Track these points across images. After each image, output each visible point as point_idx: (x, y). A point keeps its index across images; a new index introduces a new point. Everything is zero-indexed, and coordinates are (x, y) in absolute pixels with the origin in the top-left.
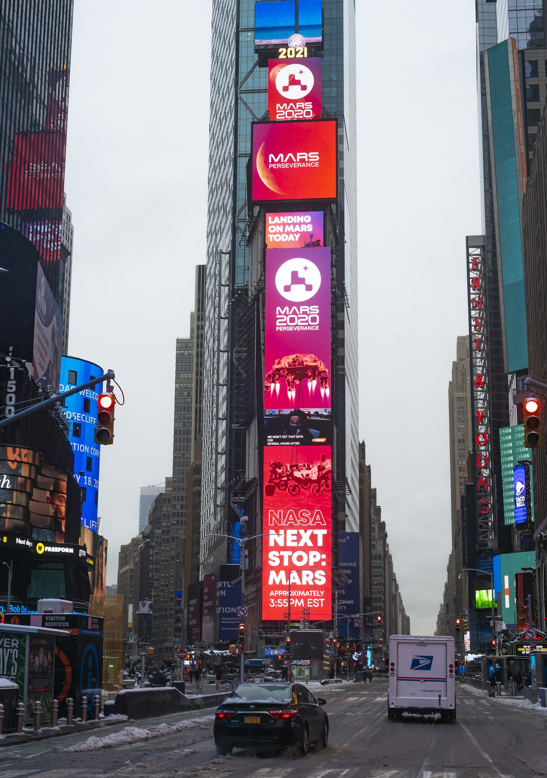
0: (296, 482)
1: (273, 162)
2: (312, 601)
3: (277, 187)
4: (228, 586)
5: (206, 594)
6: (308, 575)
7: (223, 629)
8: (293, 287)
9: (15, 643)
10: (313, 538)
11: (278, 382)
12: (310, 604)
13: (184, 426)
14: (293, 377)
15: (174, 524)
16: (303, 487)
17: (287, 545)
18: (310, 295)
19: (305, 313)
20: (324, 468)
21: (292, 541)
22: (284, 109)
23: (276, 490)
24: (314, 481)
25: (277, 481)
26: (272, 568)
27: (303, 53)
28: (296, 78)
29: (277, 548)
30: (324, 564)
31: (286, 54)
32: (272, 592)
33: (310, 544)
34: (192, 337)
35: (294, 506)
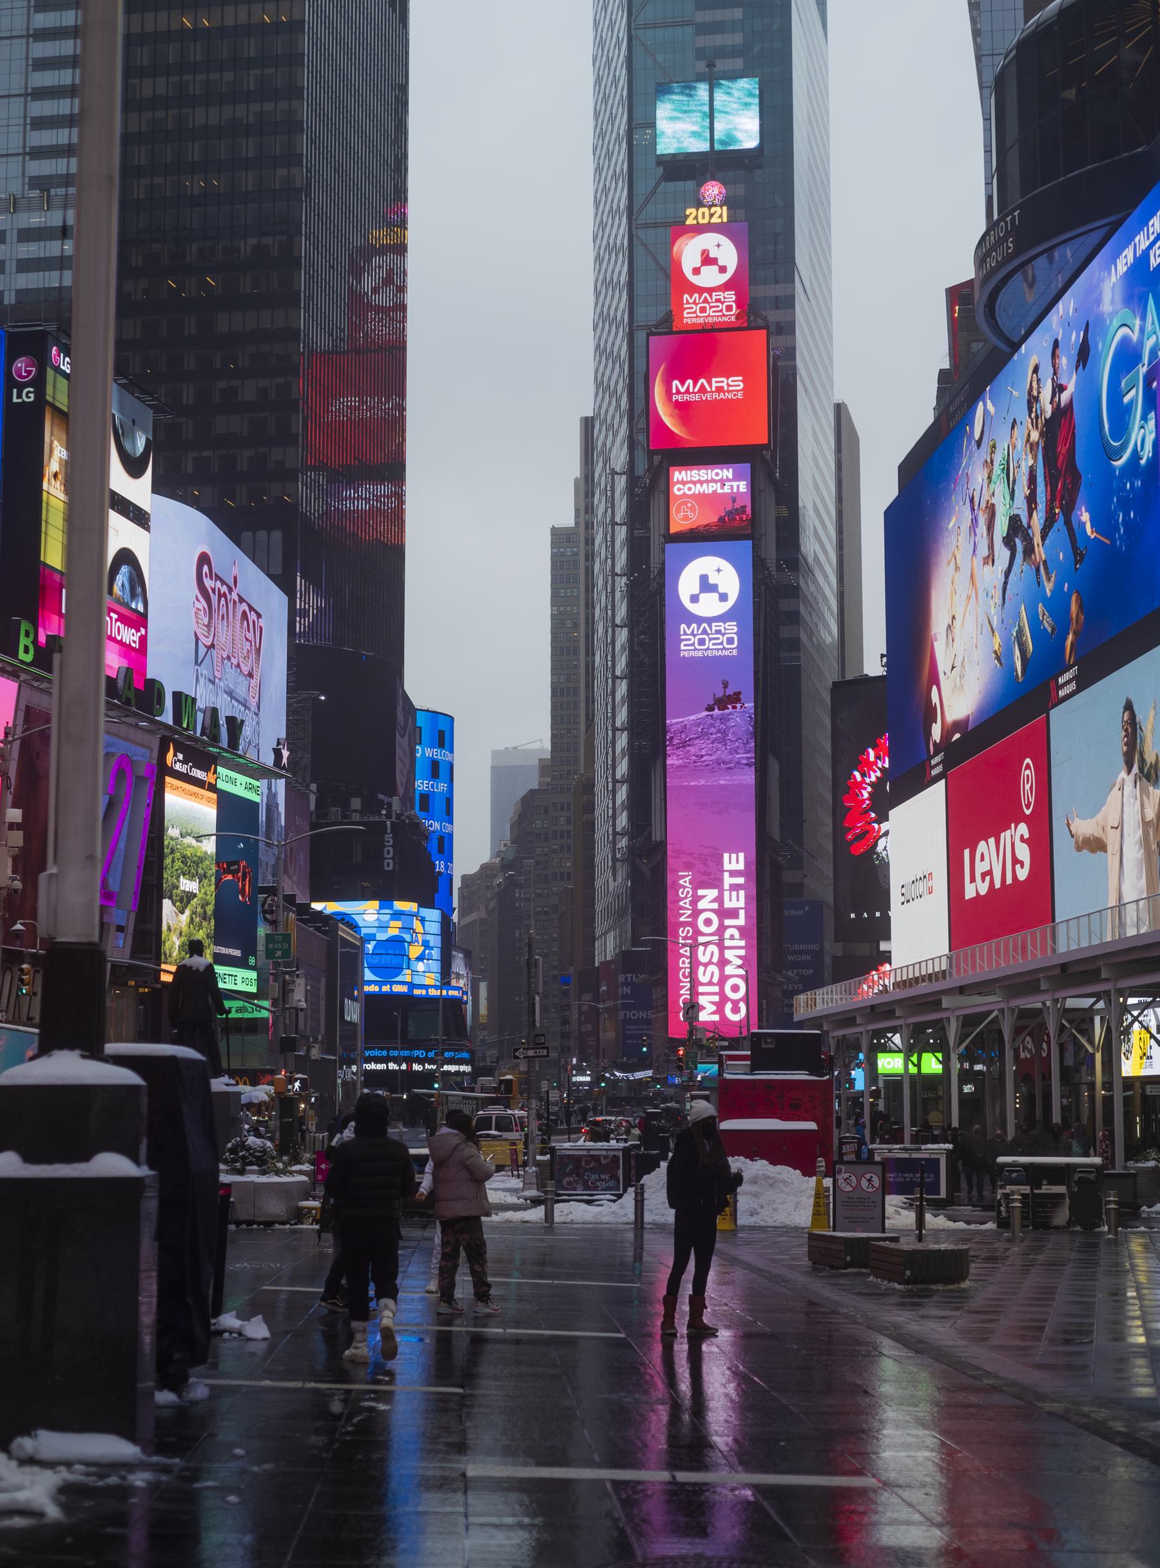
1: (678, 392)
3: (684, 429)
8: (702, 596)
9: (475, 1102)
15: (555, 851)
18: (725, 607)
19: (718, 632)
22: (694, 303)
27: (721, 216)
28: (711, 255)
31: (696, 218)
34: (577, 523)
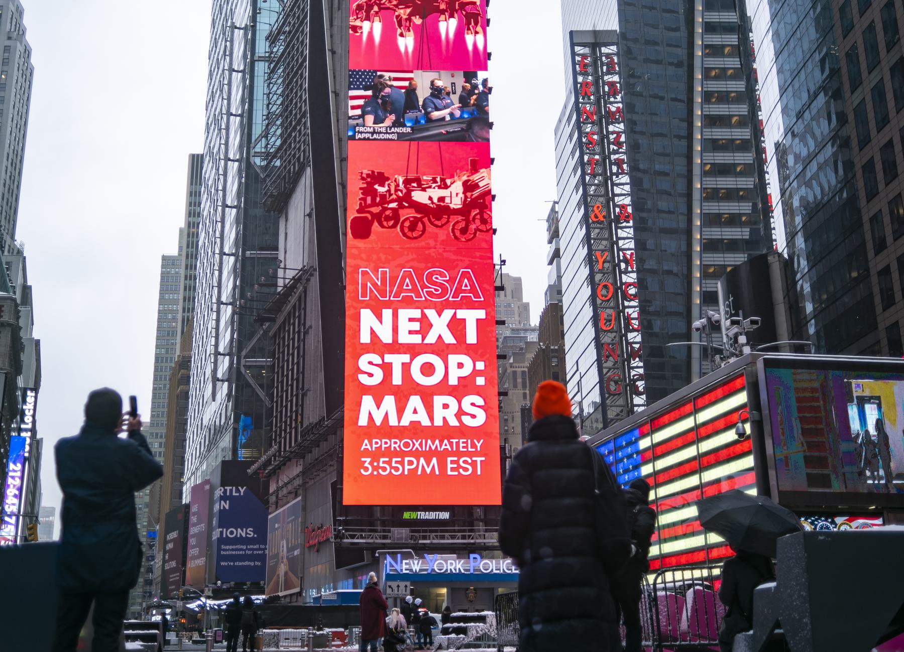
0: (417, 212)
2: (457, 462)
4: (234, 494)
5: (194, 514)
6: (446, 406)
7: (223, 564)
10: (457, 326)
11: (377, 19)
12: (452, 469)
13: (167, 352)
14: (408, 10)
16: (432, 223)
17: (401, 340)
20: (476, 186)
21: (410, 332)
23: (373, 228)
24: (456, 212)
25: (376, 210)
26: (367, 390)
29: (376, 345)
30: (480, 381)
32: (366, 441)
33: (449, 339)
35: (413, 260)
